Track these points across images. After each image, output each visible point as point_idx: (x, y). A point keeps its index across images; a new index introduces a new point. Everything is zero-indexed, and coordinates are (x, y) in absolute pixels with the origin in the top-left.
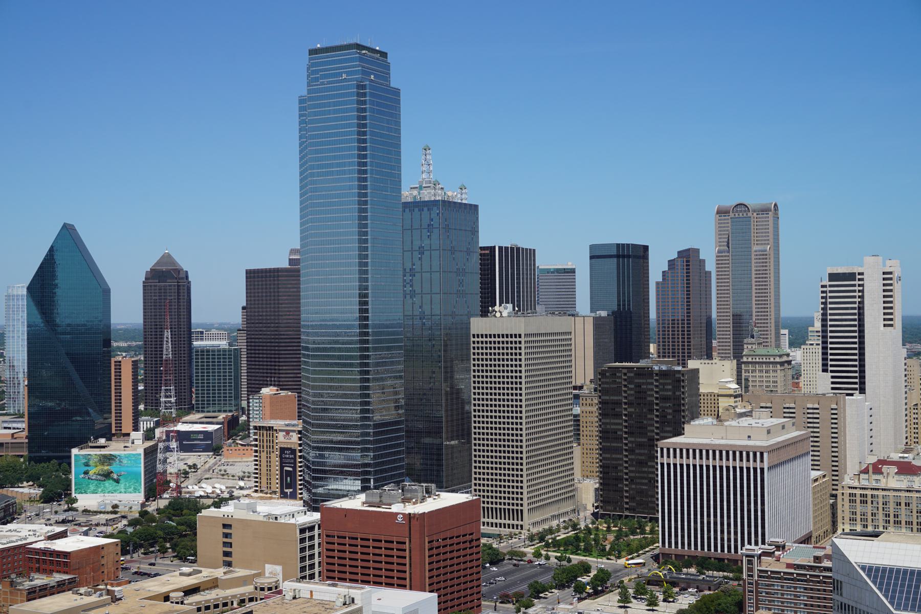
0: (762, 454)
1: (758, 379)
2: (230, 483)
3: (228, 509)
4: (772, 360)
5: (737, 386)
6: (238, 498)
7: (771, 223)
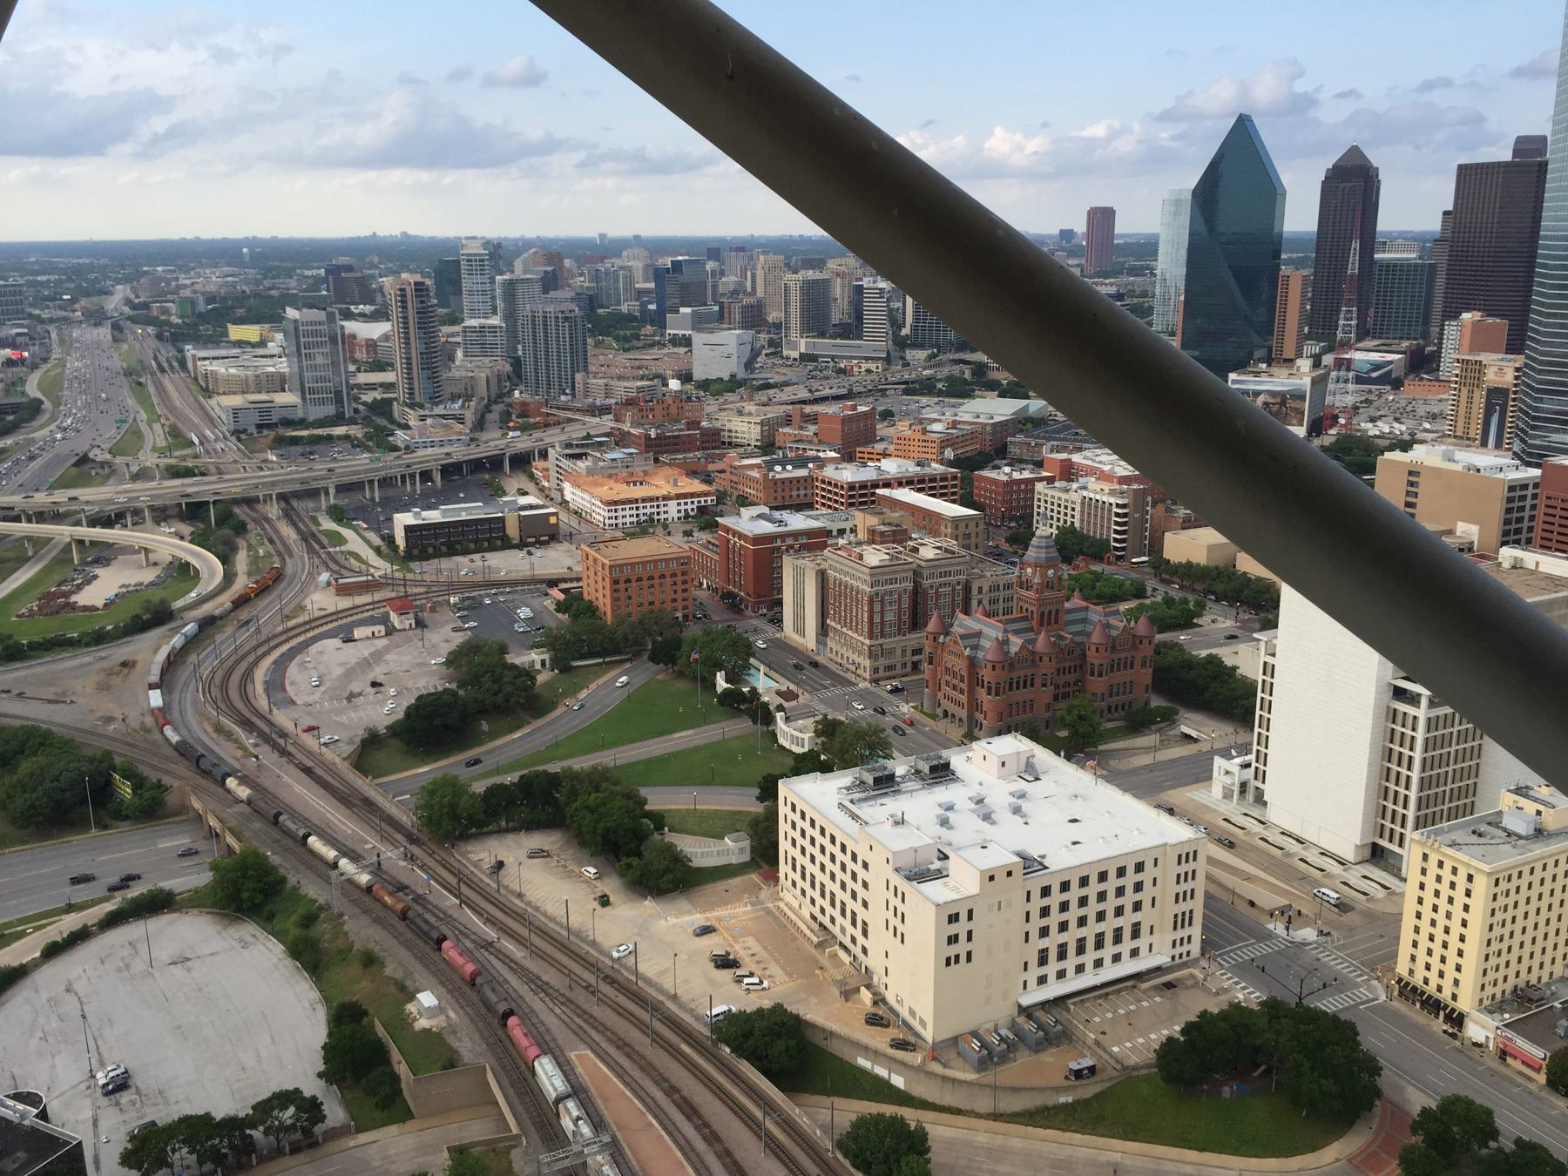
2: (1411, 423)
3: (1419, 454)
6: (1422, 442)
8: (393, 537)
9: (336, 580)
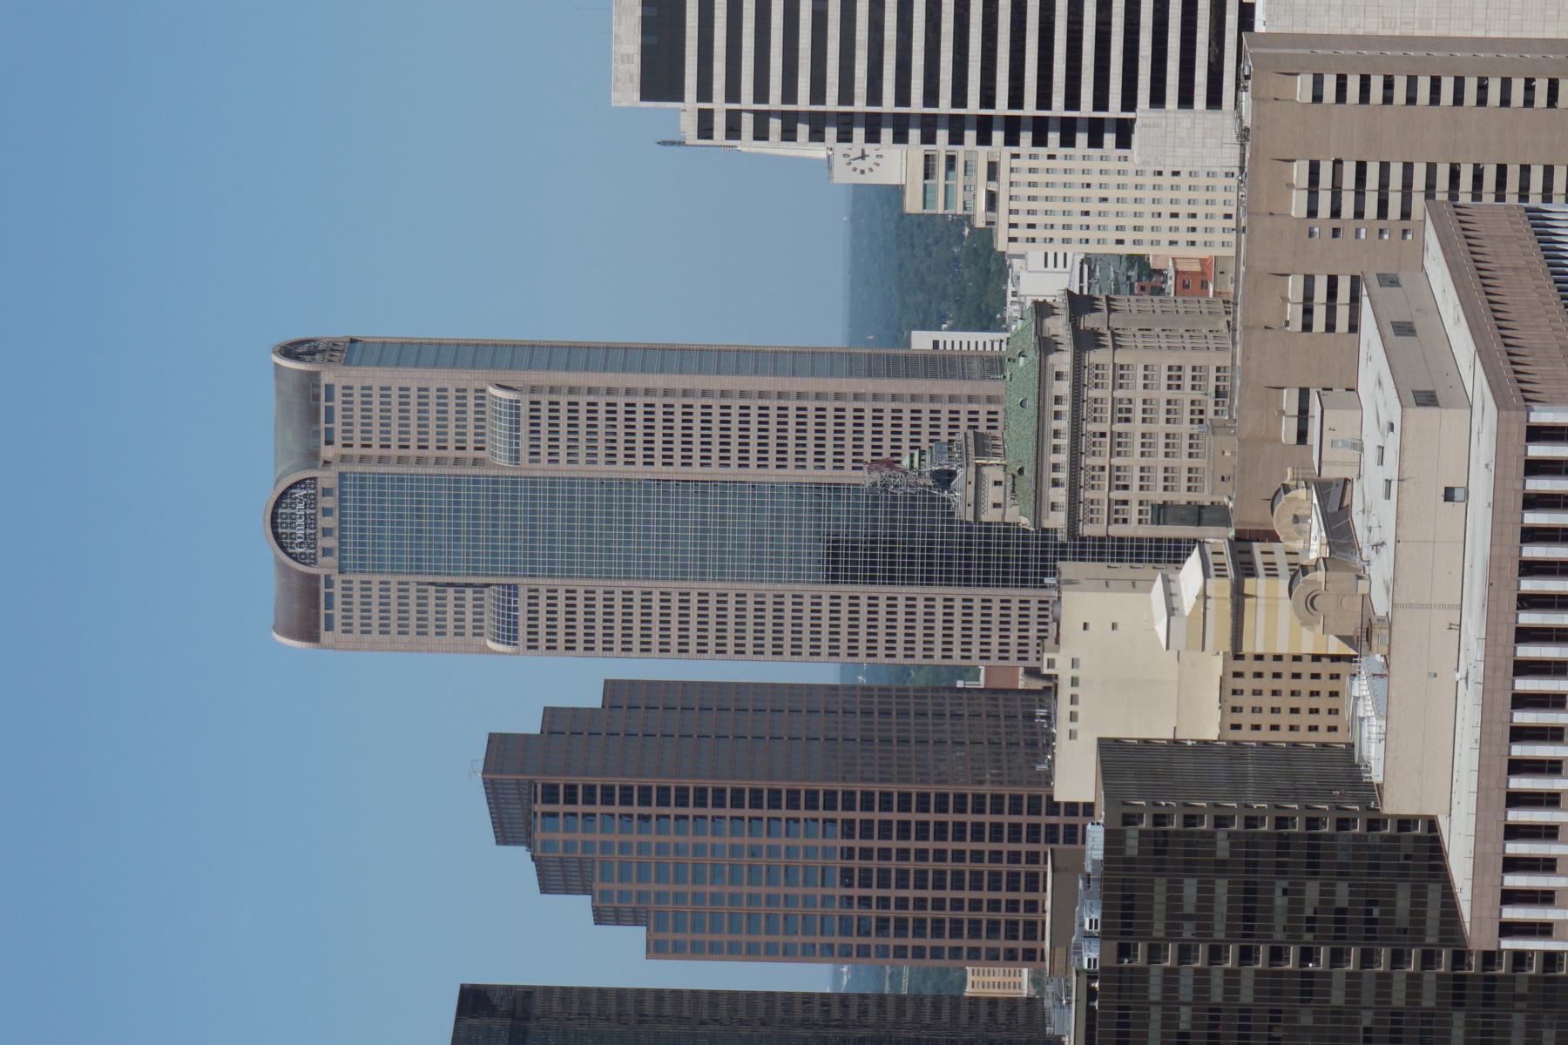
0: (1537, 433)
1: (1159, 461)
4: (1064, 388)
5: (1193, 563)
7: (376, 377)
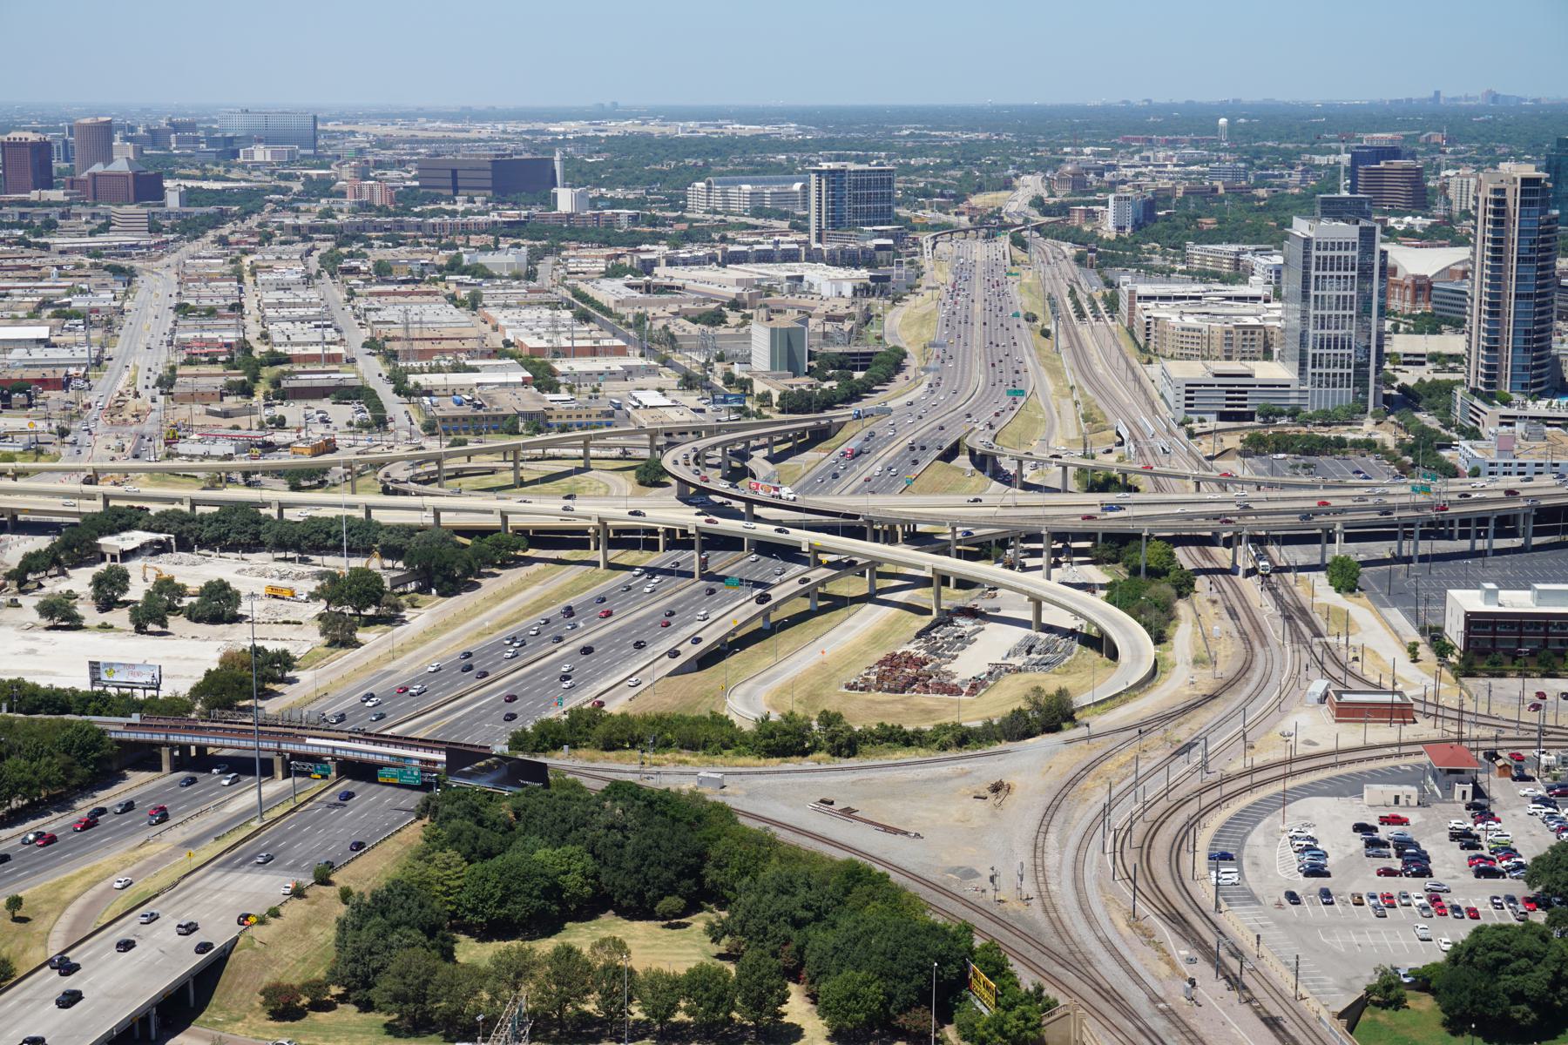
8: (1440, 629)
9: (1339, 694)
